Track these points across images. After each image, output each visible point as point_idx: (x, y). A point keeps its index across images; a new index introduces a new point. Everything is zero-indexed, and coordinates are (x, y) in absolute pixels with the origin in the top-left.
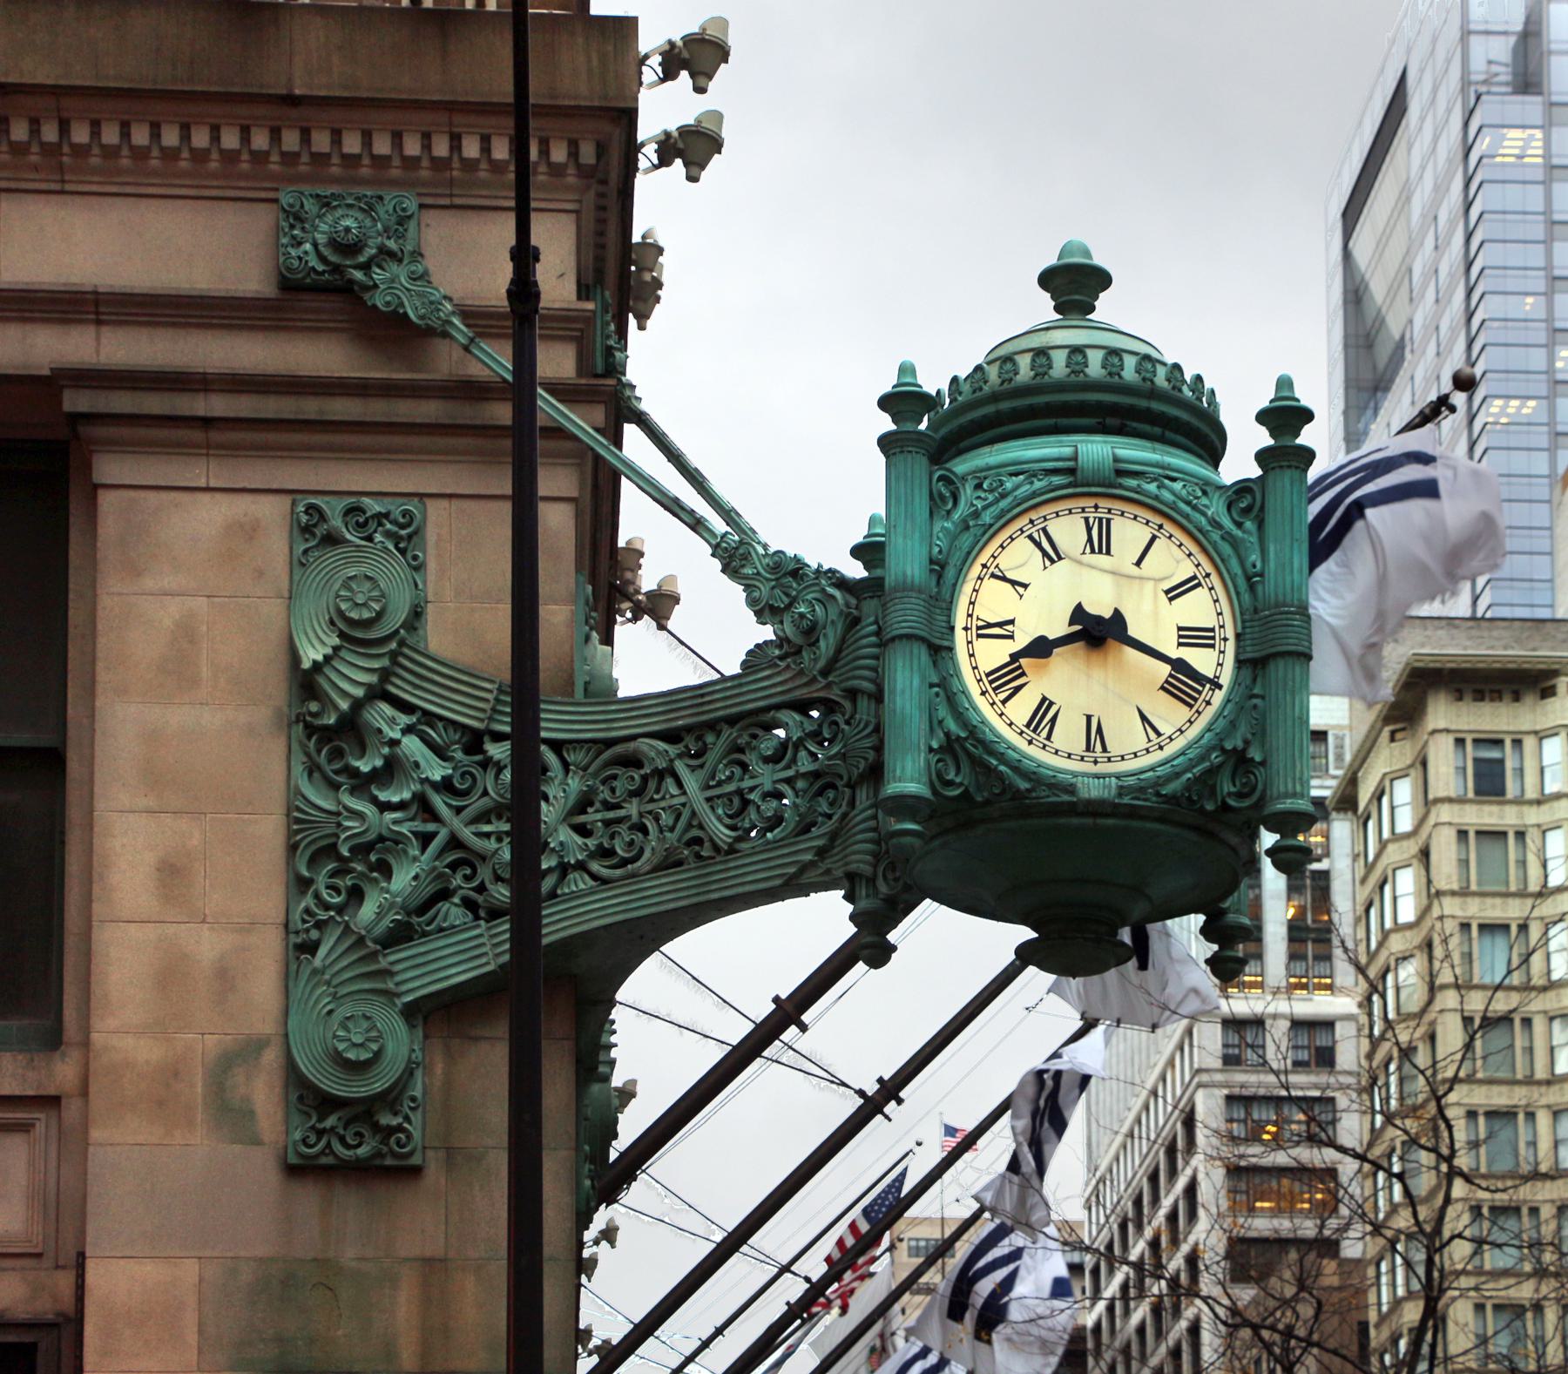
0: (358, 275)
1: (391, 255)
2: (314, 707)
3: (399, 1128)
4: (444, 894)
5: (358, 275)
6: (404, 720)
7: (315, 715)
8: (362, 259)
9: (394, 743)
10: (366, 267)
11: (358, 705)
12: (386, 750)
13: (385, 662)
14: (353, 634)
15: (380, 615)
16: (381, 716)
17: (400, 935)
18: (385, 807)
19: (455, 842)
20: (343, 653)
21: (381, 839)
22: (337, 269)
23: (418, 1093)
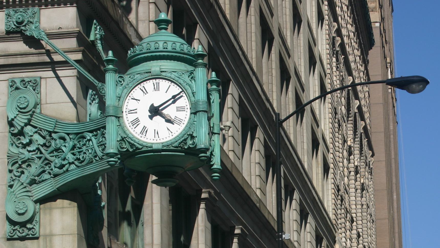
0: (23, 28)
1: (31, 22)
2: (12, 129)
3: (33, 228)
4: (44, 172)
5: (23, 28)
6: (35, 130)
7: (13, 131)
8: (24, 24)
9: (32, 136)
10: (25, 26)
11: (22, 128)
12: (30, 138)
13: (29, 117)
14: (21, 110)
15: (27, 106)
16: (28, 129)
17: (33, 182)
18: (29, 151)
19: (46, 159)
20: (19, 116)
21: (29, 159)
22: (18, 27)
23: (38, 220)
